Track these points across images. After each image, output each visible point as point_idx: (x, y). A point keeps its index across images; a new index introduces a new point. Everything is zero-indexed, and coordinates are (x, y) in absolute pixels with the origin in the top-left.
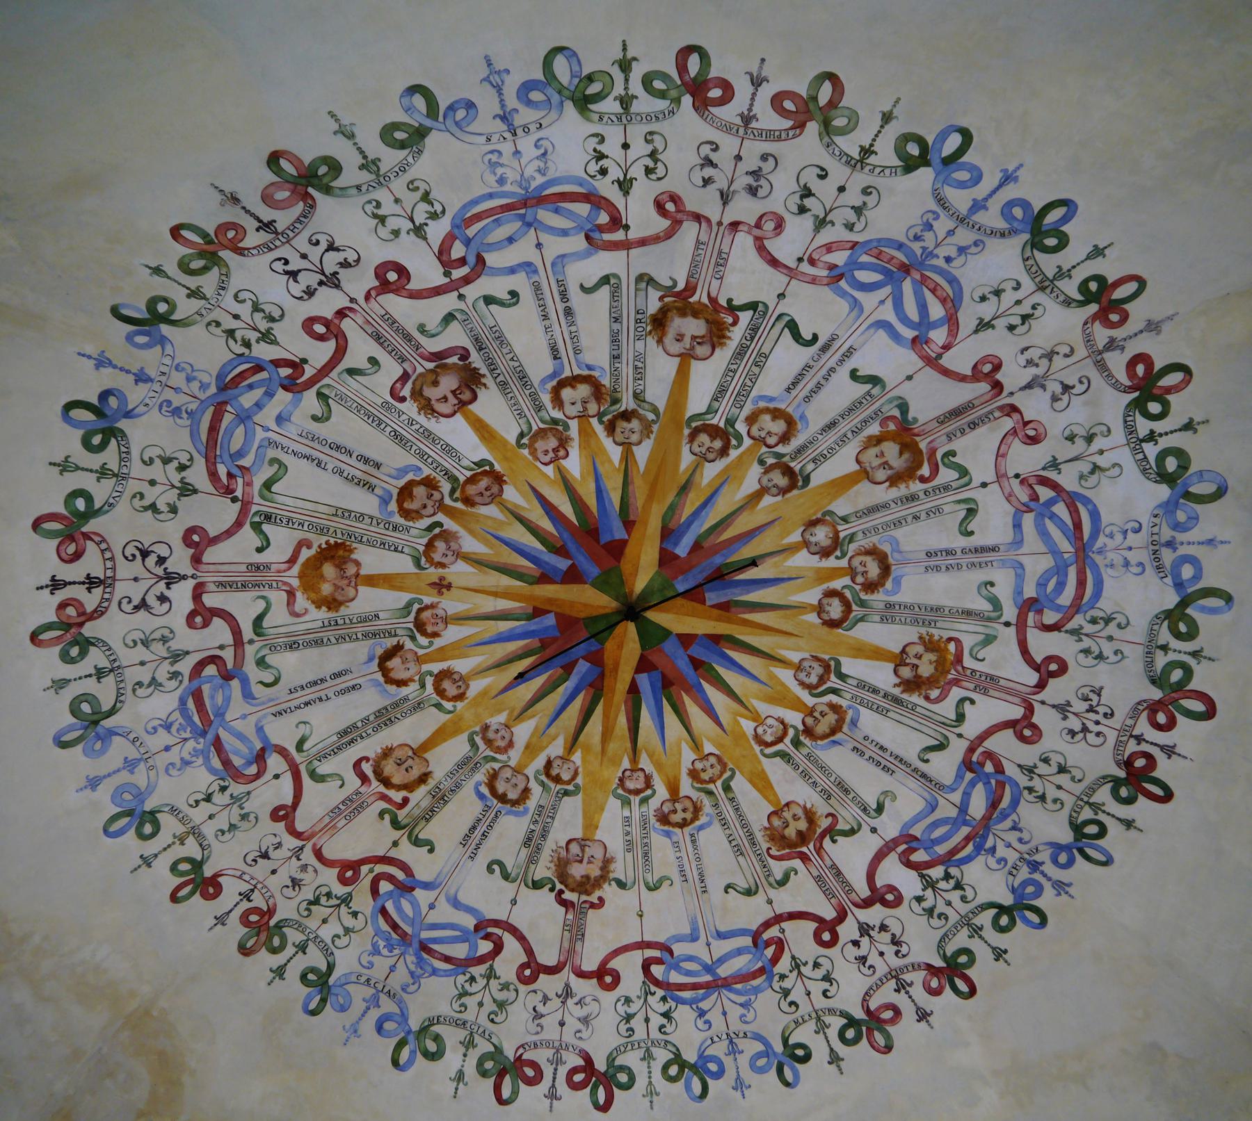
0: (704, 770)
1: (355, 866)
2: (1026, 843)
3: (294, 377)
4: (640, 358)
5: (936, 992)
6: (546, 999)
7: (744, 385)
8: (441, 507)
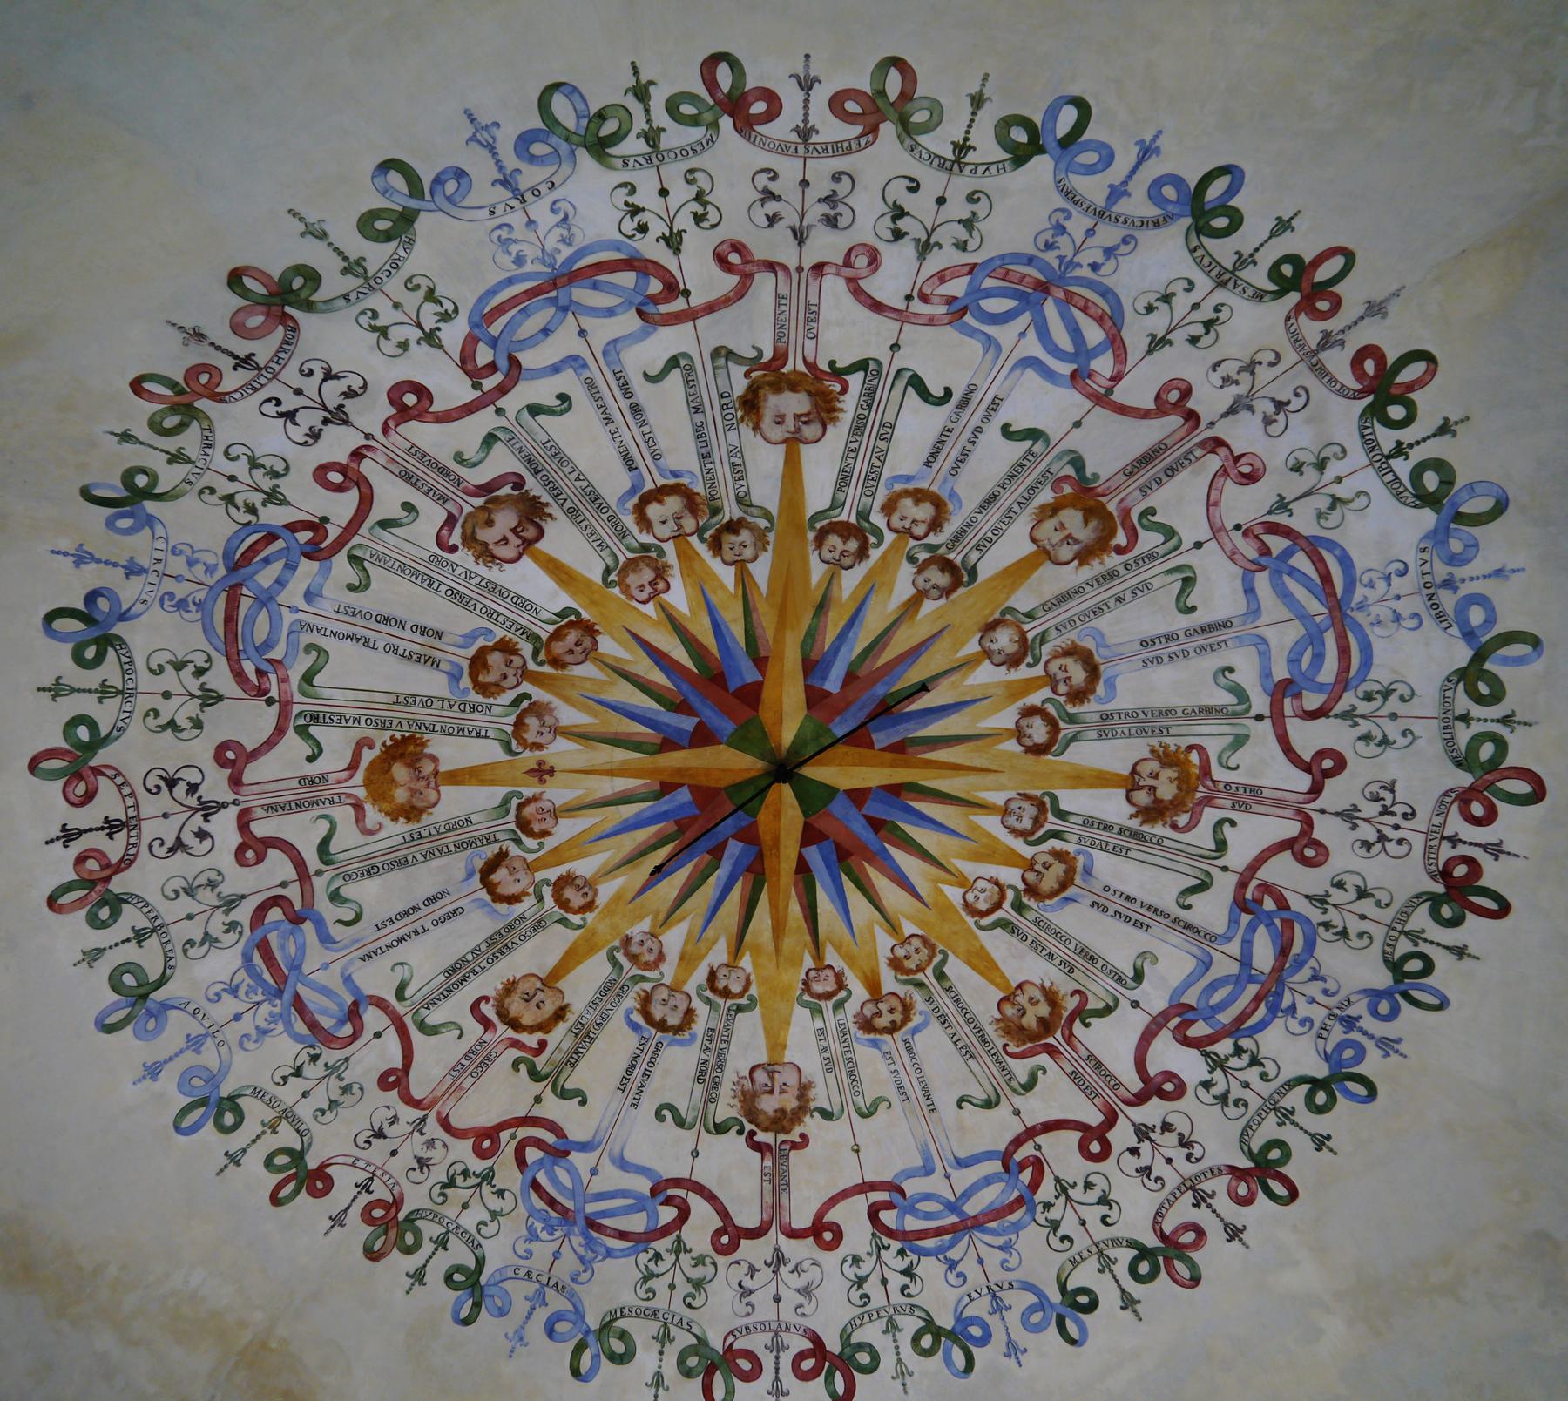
0: (907, 957)
1: (492, 1133)
2: (1334, 994)
3: (316, 541)
4: (736, 452)
5: (1247, 1201)
6: (752, 1271)
7: (871, 466)
8: (525, 674)
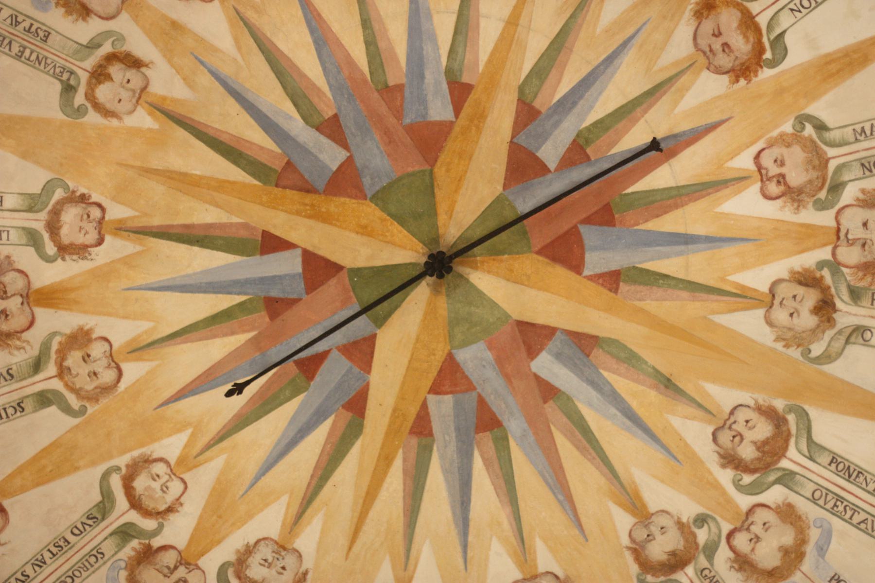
0: (86, 358)
7: (856, 509)
